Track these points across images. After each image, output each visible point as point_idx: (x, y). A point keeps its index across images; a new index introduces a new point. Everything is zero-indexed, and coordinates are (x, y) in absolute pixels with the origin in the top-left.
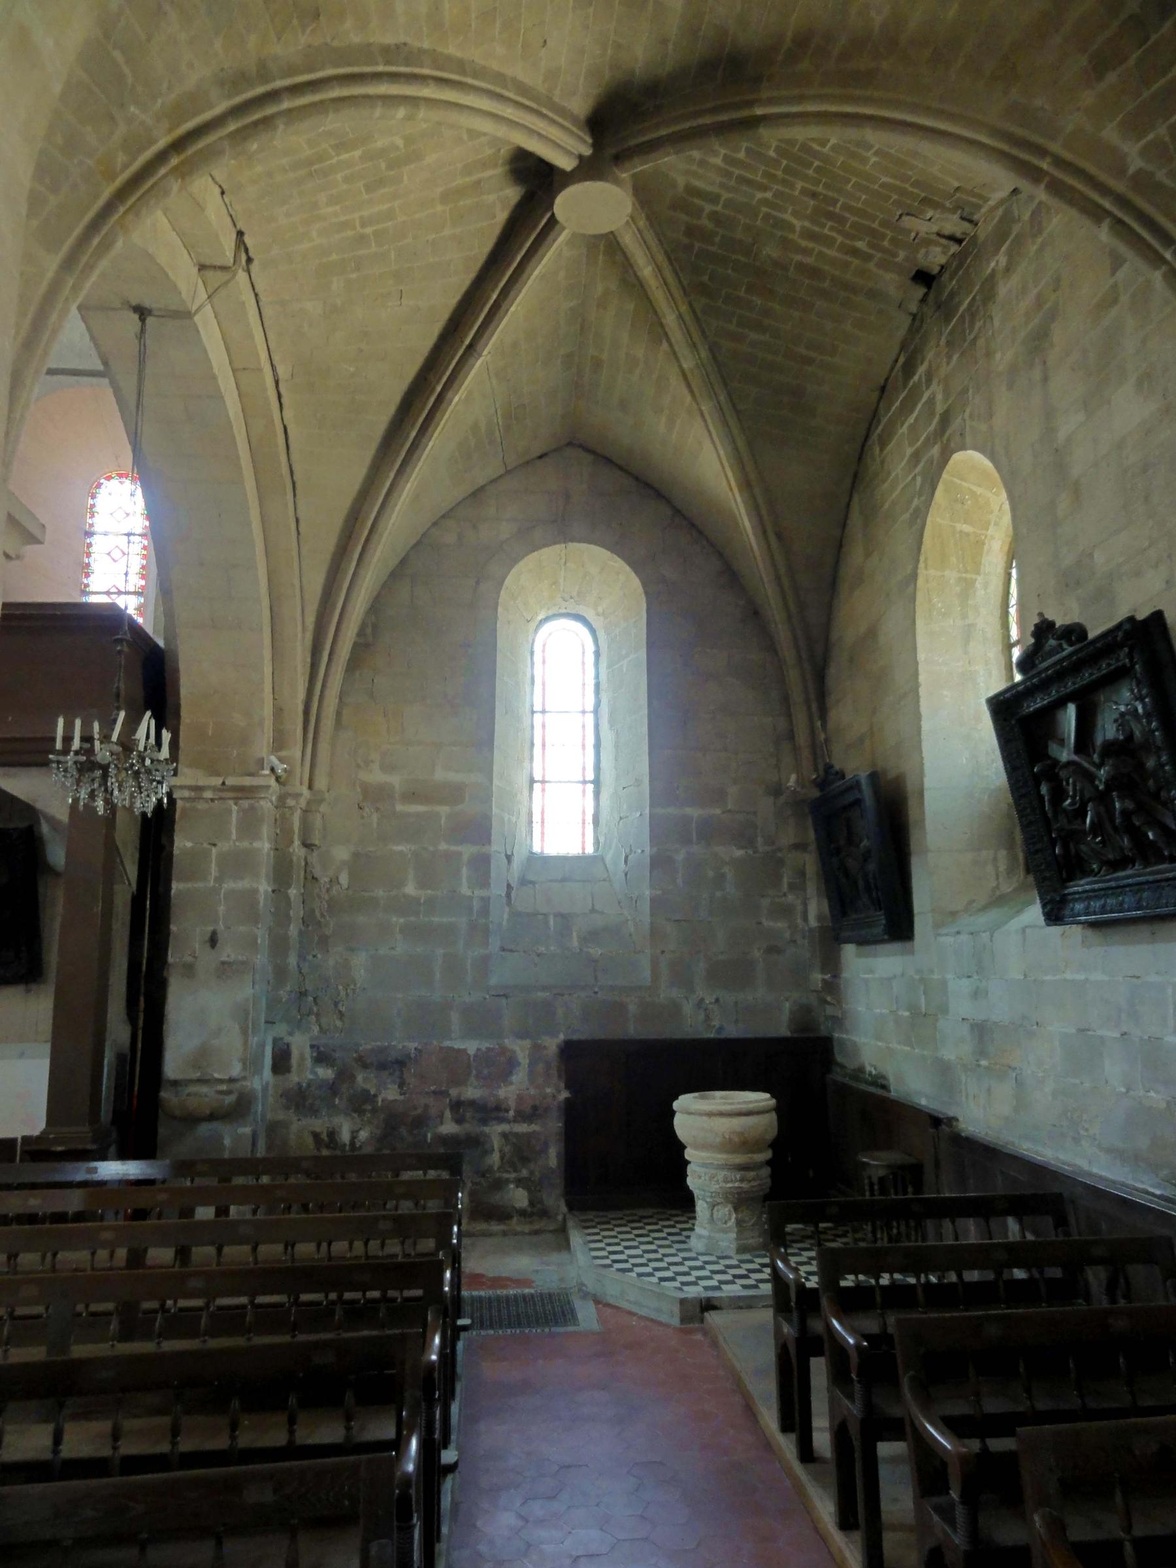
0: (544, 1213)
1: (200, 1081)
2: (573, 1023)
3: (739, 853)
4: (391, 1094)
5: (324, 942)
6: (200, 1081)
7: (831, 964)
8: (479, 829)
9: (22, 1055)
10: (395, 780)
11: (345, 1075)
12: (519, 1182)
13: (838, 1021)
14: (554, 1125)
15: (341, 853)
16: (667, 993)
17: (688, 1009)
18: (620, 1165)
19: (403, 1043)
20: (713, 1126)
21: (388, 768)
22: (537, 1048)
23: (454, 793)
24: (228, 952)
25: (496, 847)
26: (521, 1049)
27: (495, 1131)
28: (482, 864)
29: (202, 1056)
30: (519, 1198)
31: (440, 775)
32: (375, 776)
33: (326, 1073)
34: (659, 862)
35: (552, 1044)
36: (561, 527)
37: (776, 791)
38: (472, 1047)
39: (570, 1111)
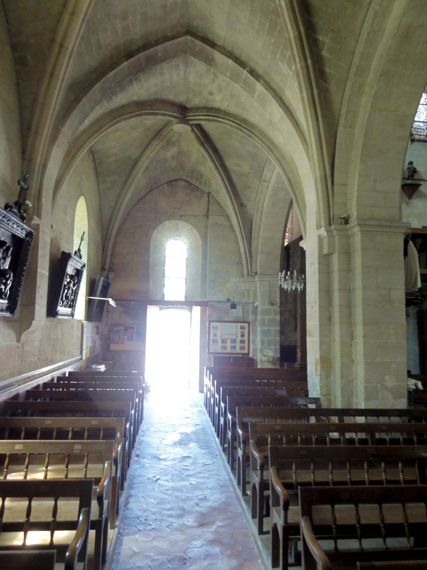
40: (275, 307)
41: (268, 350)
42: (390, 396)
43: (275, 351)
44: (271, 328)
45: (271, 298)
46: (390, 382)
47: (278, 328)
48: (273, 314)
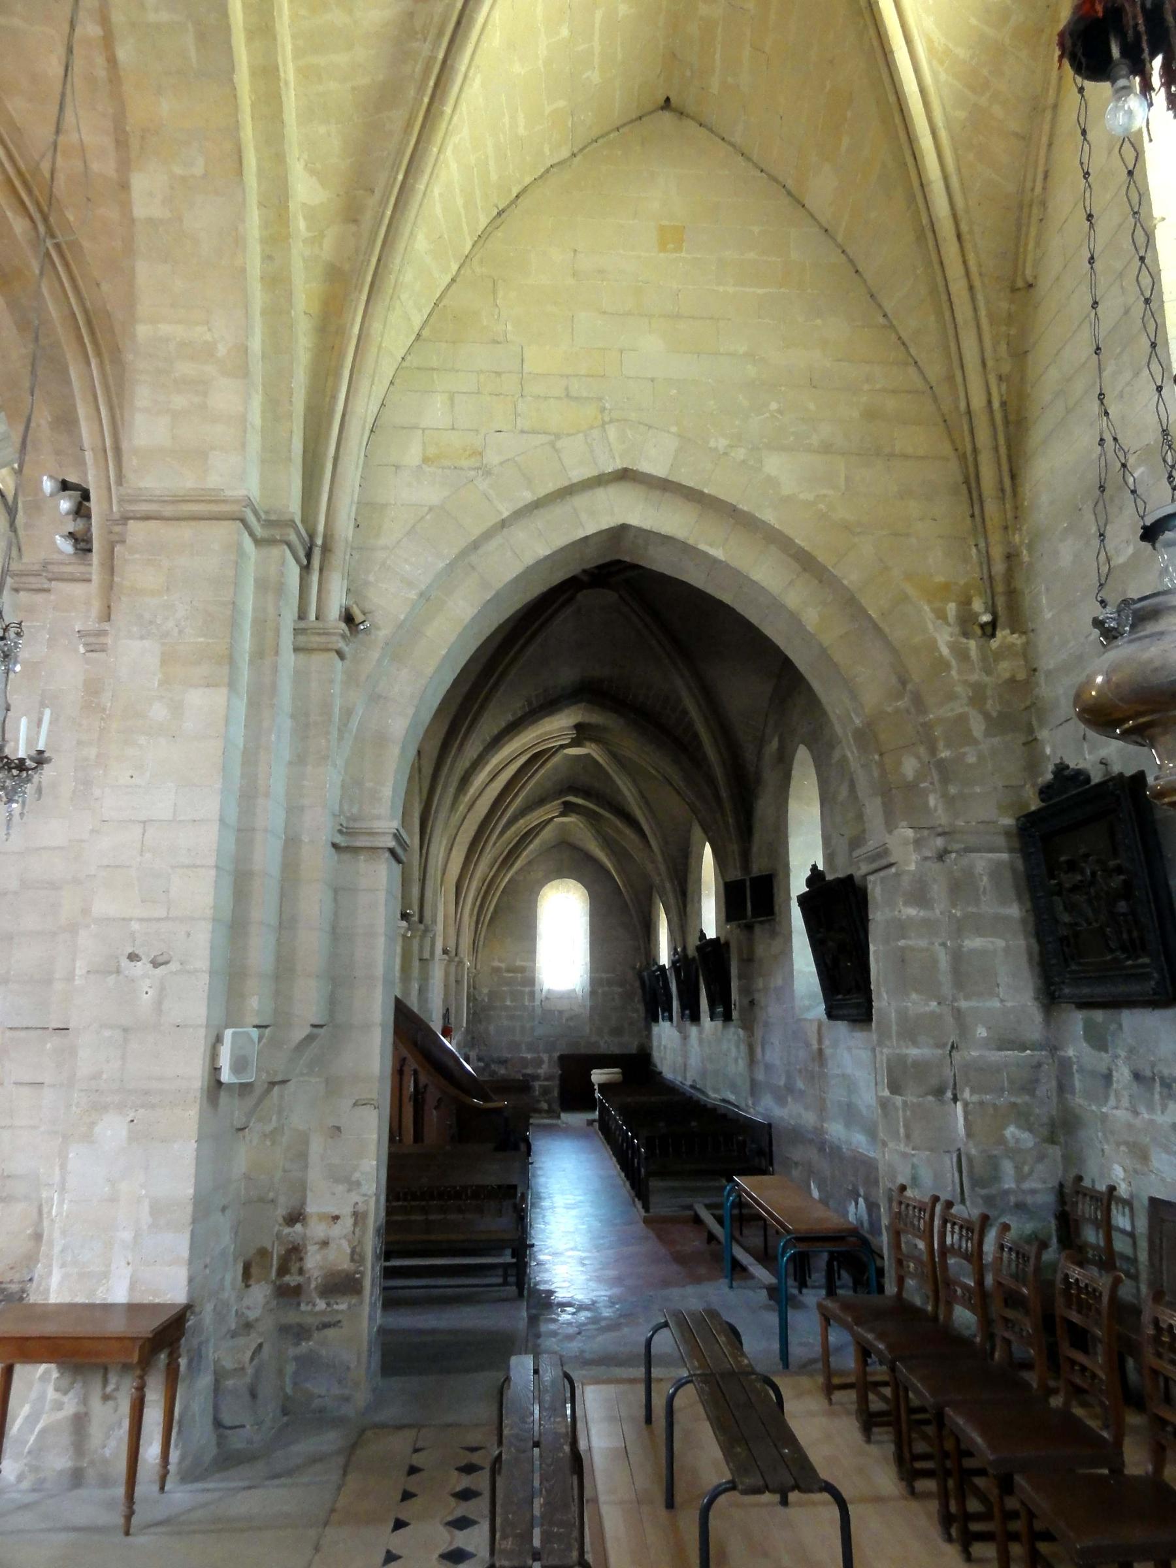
0: (554, 1111)
2: (562, 1048)
3: (620, 990)
4: (502, 1071)
5: (480, 1021)
7: (649, 1029)
8: (531, 981)
10: (503, 965)
11: (487, 1065)
12: (546, 1101)
13: (651, 1048)
14: (557, 1082)
15: (485, 991)
16: (594, 1039)
17: (602, 1043)
18: (574, 1093)
19: (506, 1054)
20: (598, 1076)
21: (500, 960)
22: (550, 1058)
23: (522, 970)
25: (537, 988)
26: (545, 1057)
27: (537, 1084)
28: (532, 994)
30: (545, 1106)
31: (518, 963)
32: (496, 964)
34: (593, 993)
35: (556, 1055)
36: (560, 873)
37: (634, 968)
38: (529, 1056)
39: (563, 1079)
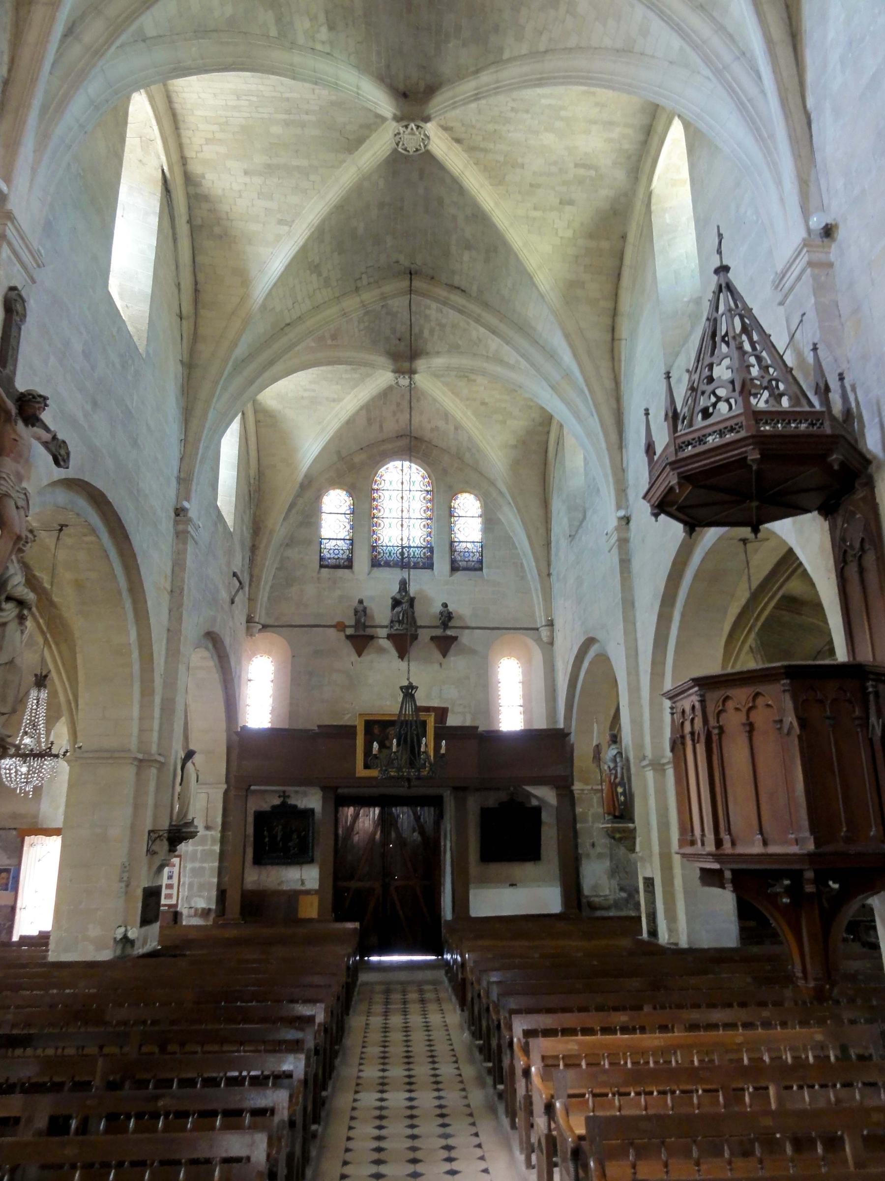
1: (596, 896)
6: (596, 896)
9: (539, 886)
24: (599, 849)
29: (595, 887)
33: (624, 895)
40: (213, 833)
41: (197, 899)
42: (91, 948)
43: (209, 899)
44: (205, 865)
45: (209, 819)
46: (94, 931)
47: (216, 864)
48: (209, 842)
